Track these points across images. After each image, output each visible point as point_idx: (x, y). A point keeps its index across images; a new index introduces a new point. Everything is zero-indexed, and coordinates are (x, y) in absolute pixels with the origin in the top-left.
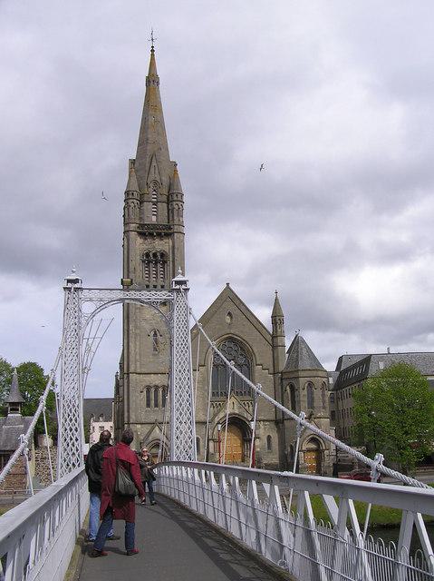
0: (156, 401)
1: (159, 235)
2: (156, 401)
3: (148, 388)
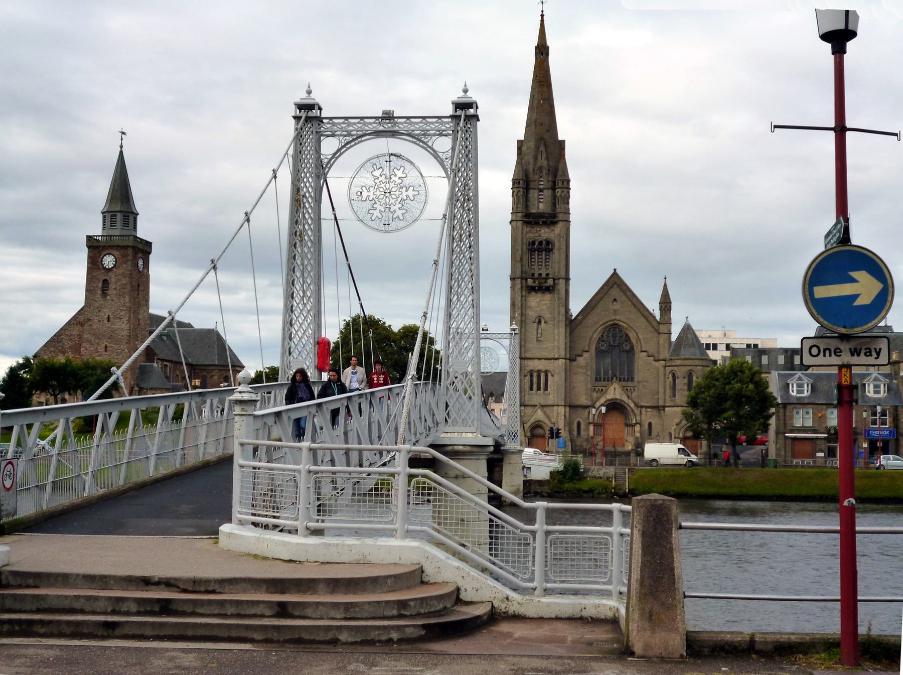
0: (539, 384)
1: (545, 223)
2: (539, 384)
3: (531, 373)
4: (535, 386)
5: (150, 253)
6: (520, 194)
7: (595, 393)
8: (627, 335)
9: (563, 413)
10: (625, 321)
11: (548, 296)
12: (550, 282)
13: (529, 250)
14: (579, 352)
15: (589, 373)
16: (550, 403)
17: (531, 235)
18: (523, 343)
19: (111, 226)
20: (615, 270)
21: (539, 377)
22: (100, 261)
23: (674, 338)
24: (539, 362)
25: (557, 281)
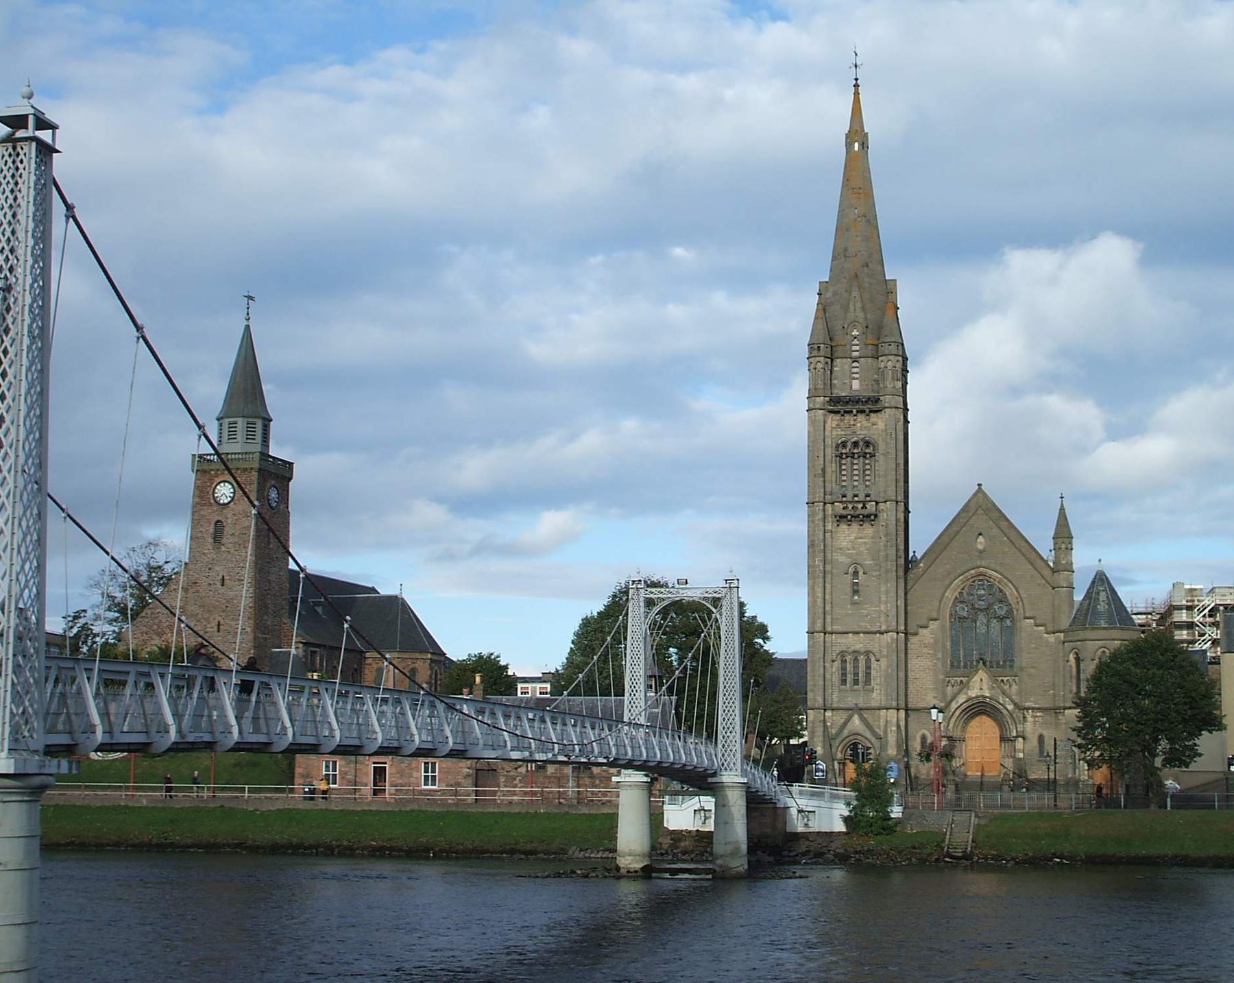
2: (856, 674)
3: (842, 654)
4: (850, 678)
5: (290, 479)
6: (820, 366)
7: (950, 688)
8: (1001, 591)
9: (895, 720)
10: (998, 568)
11: (868, 530)
12: (871, 507)
13: (837, 456)
14: (924, 622)
15: (940, 655)
16: (874, 704)
17: (840, 432)
18: (828, 608)
19: (247, 439)
20: (980, 485)
21: (856, 660)
22: (211, 493)
23: (1079, 597)
24: (856, 637)
25: (881, 506)
